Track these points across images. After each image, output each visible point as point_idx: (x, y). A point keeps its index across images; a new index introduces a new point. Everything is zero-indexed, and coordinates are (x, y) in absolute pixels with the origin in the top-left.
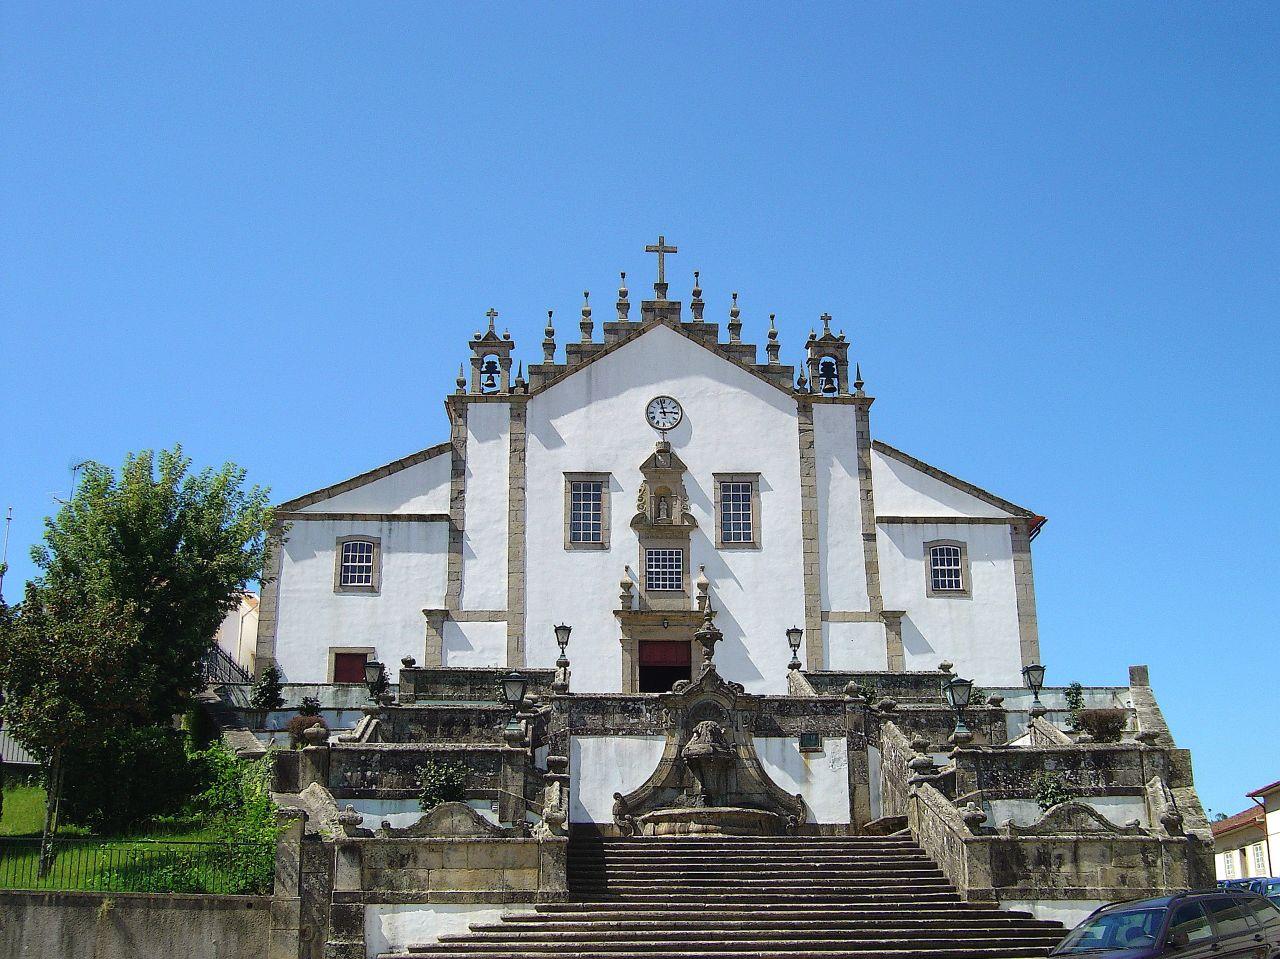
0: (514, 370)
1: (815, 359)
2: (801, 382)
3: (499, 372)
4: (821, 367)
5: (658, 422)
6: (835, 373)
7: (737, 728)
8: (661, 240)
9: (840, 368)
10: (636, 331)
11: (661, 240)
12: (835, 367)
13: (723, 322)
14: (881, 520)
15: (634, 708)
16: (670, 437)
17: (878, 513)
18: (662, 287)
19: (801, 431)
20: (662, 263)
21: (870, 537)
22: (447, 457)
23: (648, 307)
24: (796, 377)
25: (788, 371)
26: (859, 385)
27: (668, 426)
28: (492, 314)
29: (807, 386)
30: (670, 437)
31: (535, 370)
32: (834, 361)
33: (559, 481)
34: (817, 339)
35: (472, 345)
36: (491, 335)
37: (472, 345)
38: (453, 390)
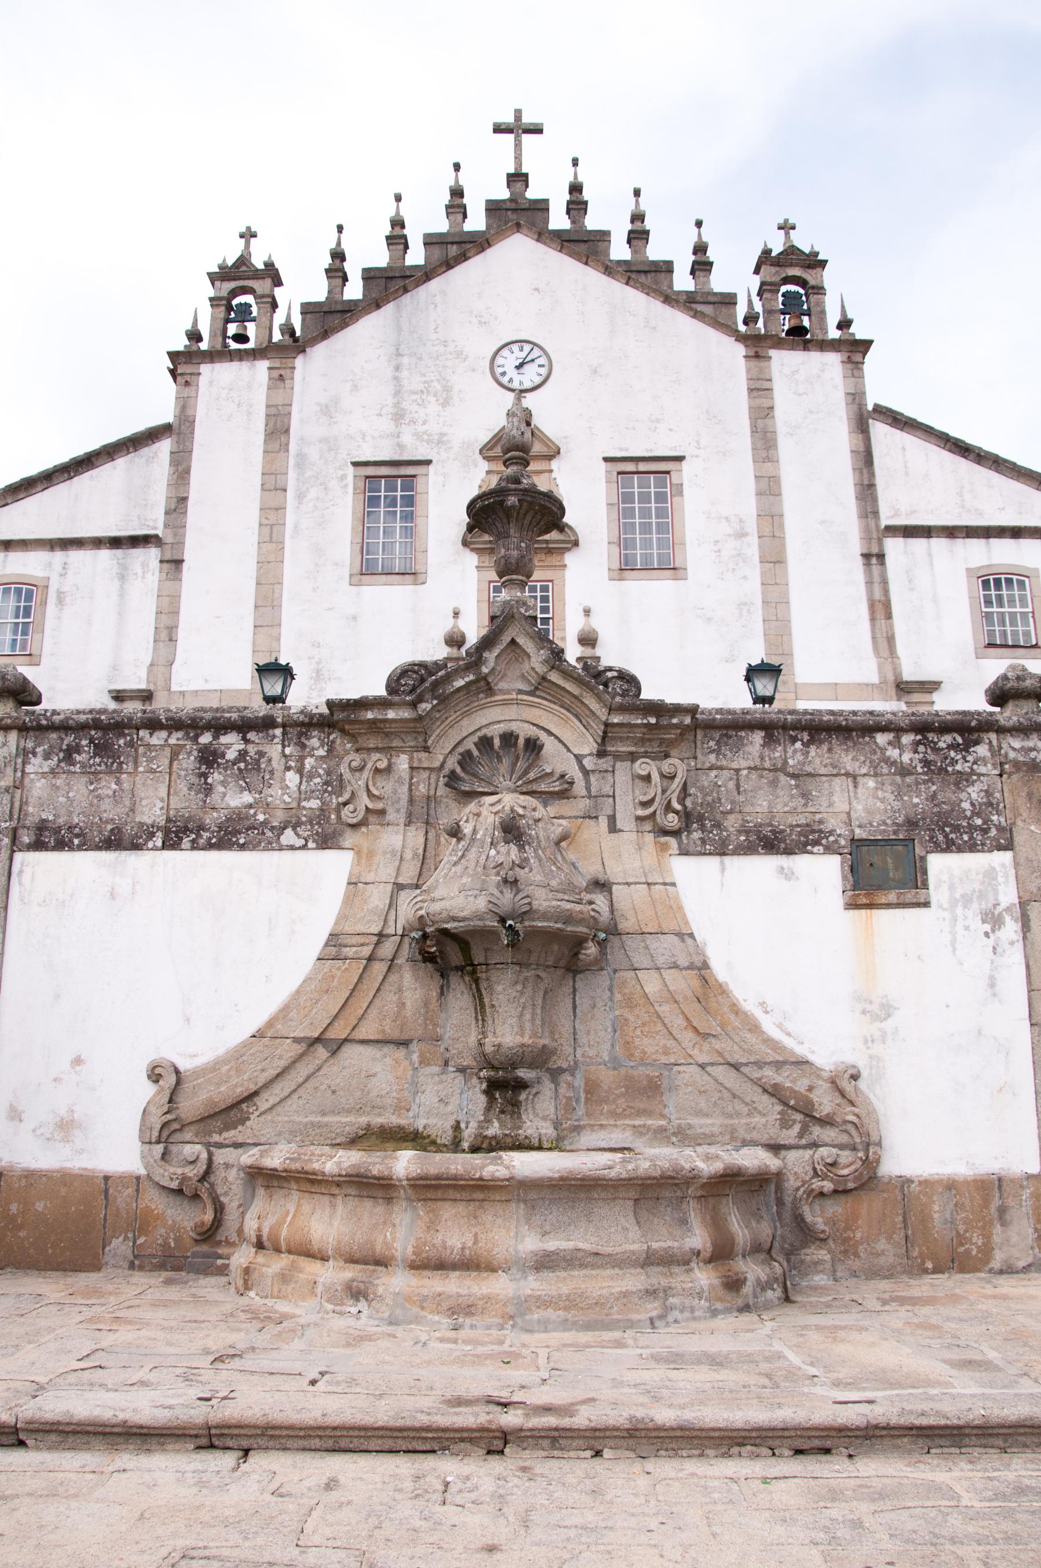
0: (279, 318)
1: (771, 284)
2: (750, 319)
3: (254, 320)
4: (781, 299)
5: (511, 380)
6: (805, 307)
7: (612, 819)
8: (518, 114)
9: (813, 298)
10: (479, 243)
11: (518, 114)
12: (804, 298)
13: (619, 231)
14: (893, 531)
15: (242, 755)
16: (530, 401)
17: (884, 522)
18: (518, 179)
19: (751, 390)
20: (518, 145)
21: (873, 558)
22: (164, 447)
23: (493, 208)
24: (741, 311)
25: (729, 300)
26: (844, 324)
27: (528, 385)
28: (249, 235)
29: (760, 324)
30: (530, 401)
31: (308, 309)
32: (802, 291)
33: (343, 477)
34: (774, 254)
35: (213, 278)
36: (243, 261)
37: (213, 278)
38: (180, 343)
